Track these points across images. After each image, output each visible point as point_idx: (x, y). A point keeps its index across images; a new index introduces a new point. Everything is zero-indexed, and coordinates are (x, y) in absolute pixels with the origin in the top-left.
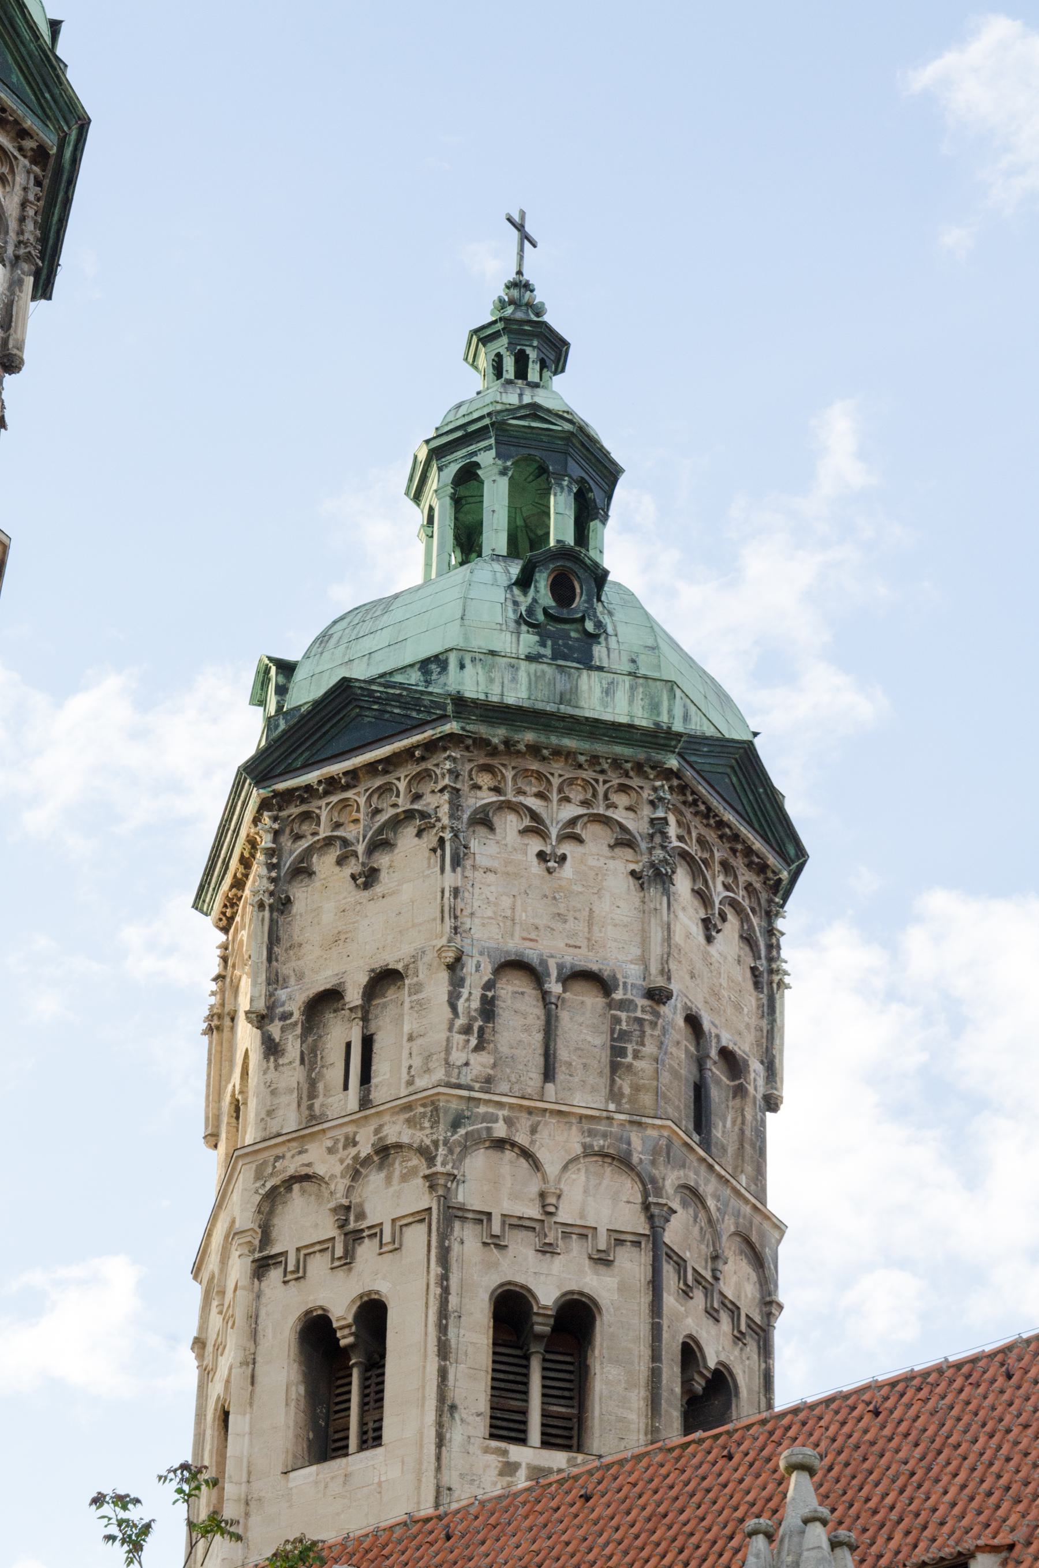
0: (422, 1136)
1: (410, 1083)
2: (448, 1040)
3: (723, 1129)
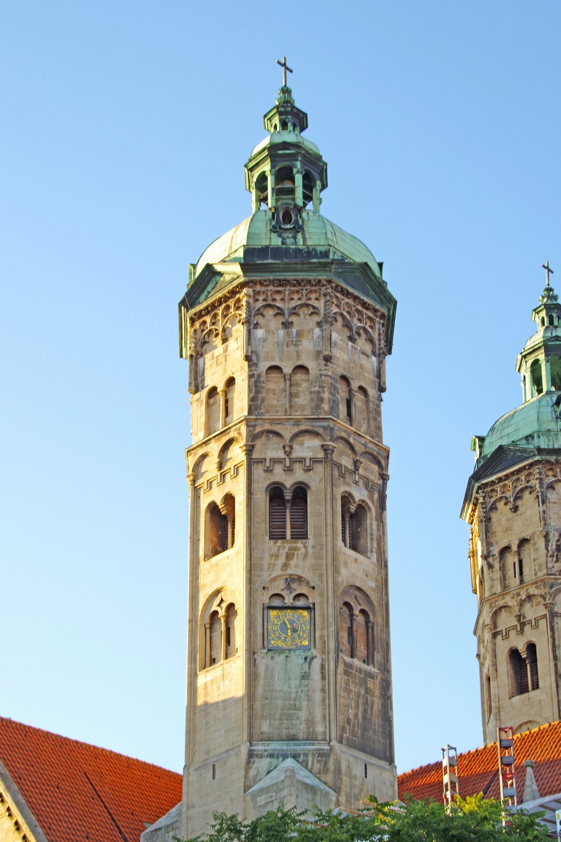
0: (542, 591)
1: (536, 574)
2: (546, 560)
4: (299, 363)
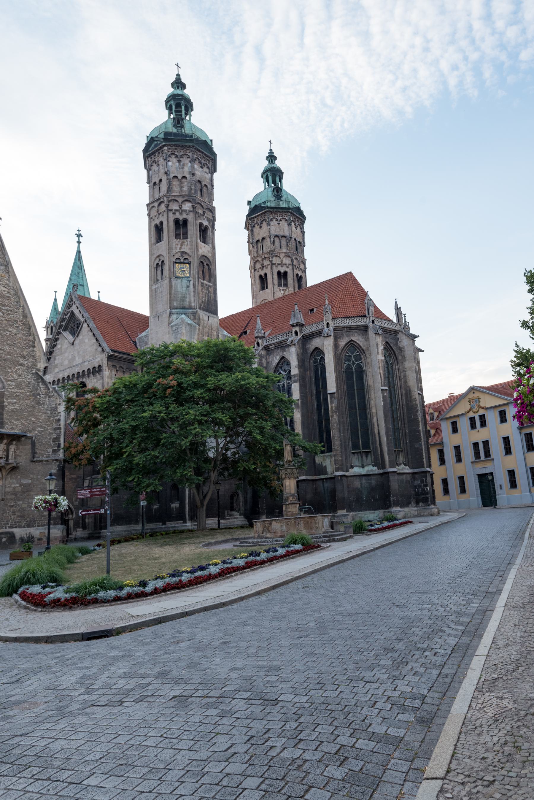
3: (299, 250)
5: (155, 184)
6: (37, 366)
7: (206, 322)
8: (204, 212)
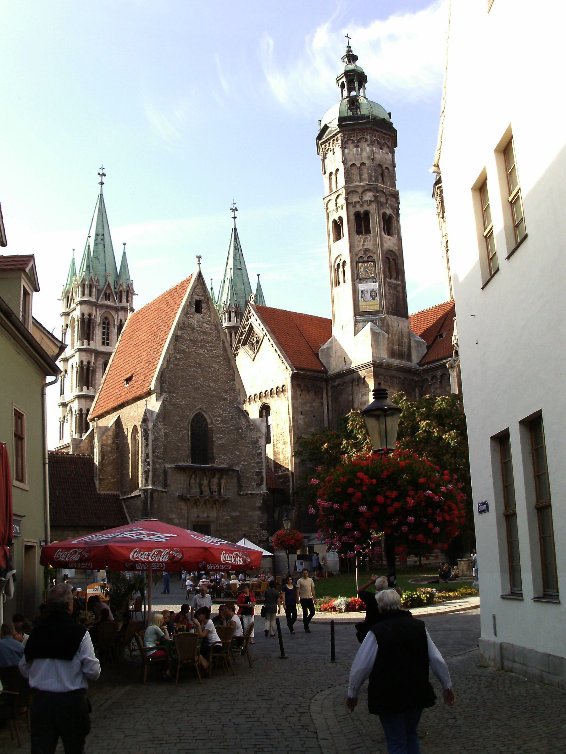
4: (362, 162)
5: (331, 174)
6: (237, 399)
7: (395, 329)
8: (387, 200)
